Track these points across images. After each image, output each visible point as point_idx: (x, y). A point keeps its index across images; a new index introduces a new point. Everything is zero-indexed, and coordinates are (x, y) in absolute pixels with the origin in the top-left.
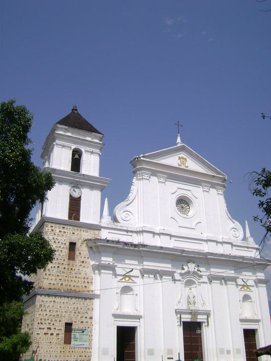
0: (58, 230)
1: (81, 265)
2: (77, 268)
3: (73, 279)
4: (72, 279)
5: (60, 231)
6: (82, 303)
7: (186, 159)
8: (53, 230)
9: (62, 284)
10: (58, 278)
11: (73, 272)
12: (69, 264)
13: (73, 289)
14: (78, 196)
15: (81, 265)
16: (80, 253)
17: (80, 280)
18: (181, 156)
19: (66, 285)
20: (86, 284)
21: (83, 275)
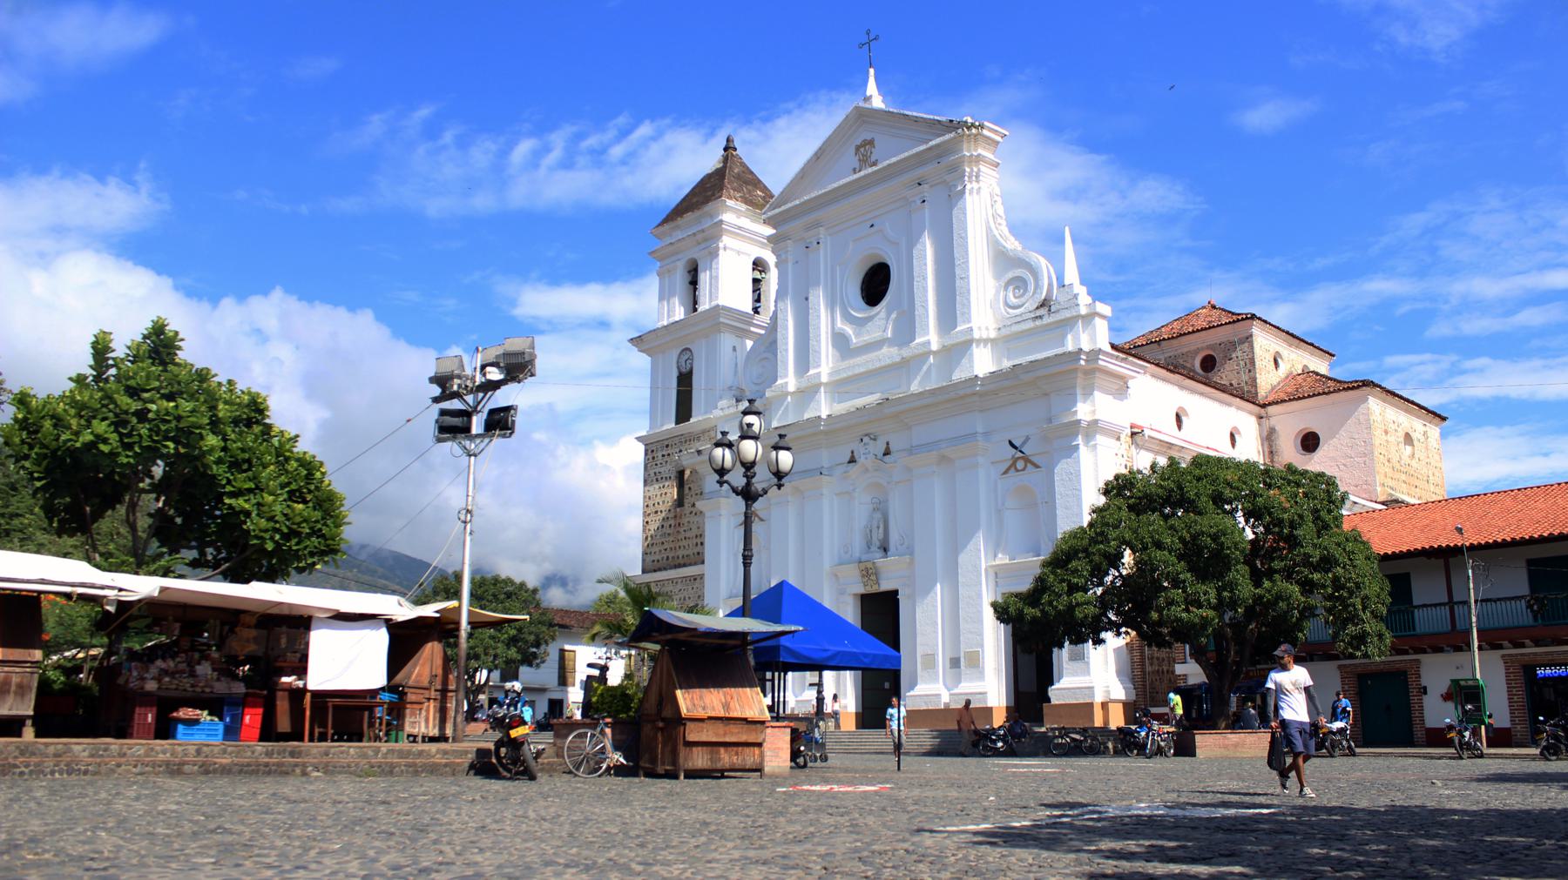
0: (660, 454)
1: (691, 513)
2: (687, 520)
3: (681, 544)
4: (681, 544)
5: (663, 456)
6: (690, 588)
7: (871, 143)
8: (653, 458)
9: (668, 558)
10: (662, 548)
11: (682, 530)
12: (675, 517)
13: (682, 562)
14: (689, 366)
15: (691, 513)
16: (690, 489)
17: (690, 542)
18: (858, 142)
19: (673, 558)
20: (699, 549)
21: (695, 532)
